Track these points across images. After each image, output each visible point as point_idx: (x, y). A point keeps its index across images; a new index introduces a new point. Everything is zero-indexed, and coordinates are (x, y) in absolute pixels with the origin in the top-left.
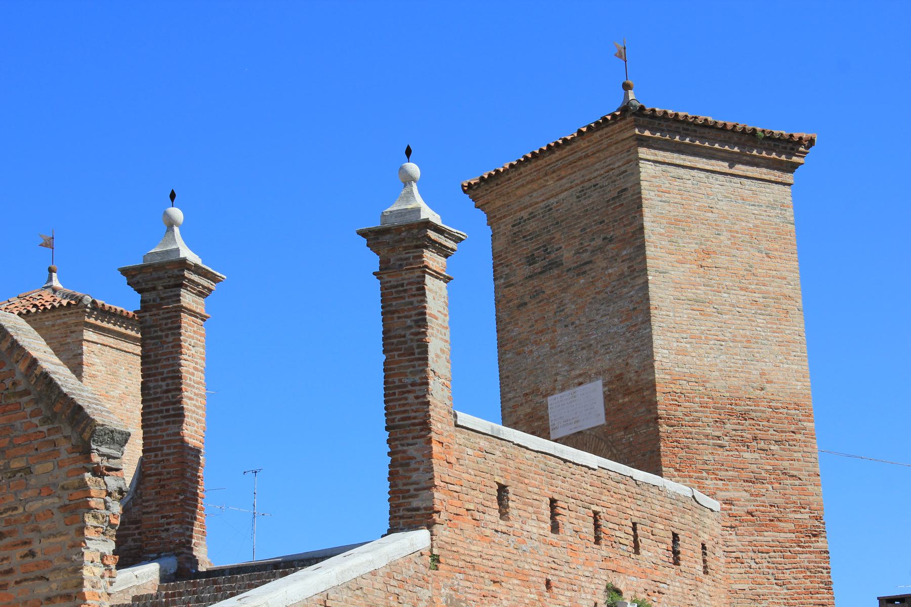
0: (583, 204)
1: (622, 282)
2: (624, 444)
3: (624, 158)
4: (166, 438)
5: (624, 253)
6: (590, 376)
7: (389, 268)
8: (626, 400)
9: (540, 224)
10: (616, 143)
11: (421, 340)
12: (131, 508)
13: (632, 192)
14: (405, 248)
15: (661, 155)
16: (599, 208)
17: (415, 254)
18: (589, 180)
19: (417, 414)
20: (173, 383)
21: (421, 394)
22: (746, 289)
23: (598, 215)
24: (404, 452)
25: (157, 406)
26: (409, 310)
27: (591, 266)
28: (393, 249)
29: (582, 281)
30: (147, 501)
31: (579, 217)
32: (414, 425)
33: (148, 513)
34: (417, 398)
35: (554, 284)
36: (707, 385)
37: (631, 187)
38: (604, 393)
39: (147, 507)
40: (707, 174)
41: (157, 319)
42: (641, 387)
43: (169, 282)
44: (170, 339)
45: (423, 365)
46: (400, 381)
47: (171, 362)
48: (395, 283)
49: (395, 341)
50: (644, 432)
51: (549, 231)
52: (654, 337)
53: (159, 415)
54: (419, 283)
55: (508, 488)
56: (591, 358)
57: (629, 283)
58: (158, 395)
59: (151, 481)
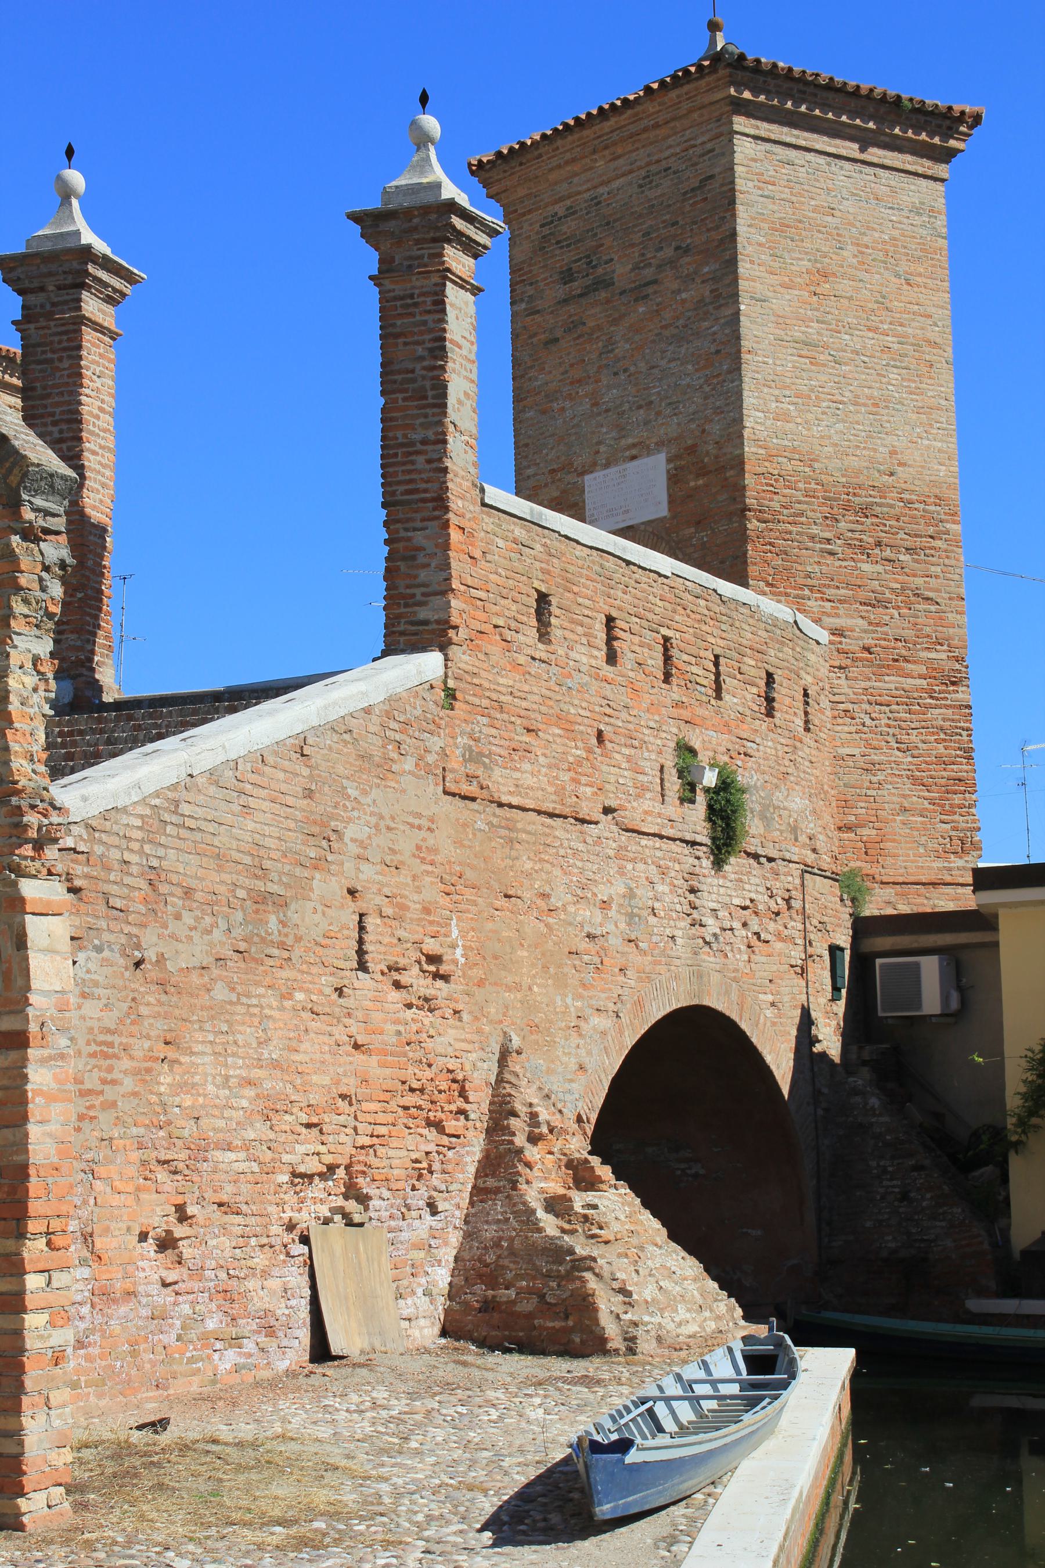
3: (711, 129)
5: (706, 270)
6: (648, 447)
8: (701, 482)
9: (582, 224)
10: (700, 108)
11: (437, 378)
14: (417, 242)
15: (765, 129)
16: (670, 202)
17: (432, 251)
18: (658, 161)
19: (429, 485)
20: (69, 429)
21: (435, 456)
22: (875, 330)
23: (668, 213)
24: (409, 539)
26: (421, 333)
27: (655, 287)
29: (641, 310)
31: (640, 216)
32: (424, 501)
36: (816, 465)
37: (720, 173)
38: (668, 471)
40: (828, 159)
43: (65, 279)
44: (66, 364)
45: (439, 414)
46: (405, 436)
47: (66, 398)
48: (401, 293)
49: (399, 377)
50: (725, 530)
51: (596, 235)
52: (745, 393)
54: (436, 294)
55: (550, 598)
56: (650, 421)
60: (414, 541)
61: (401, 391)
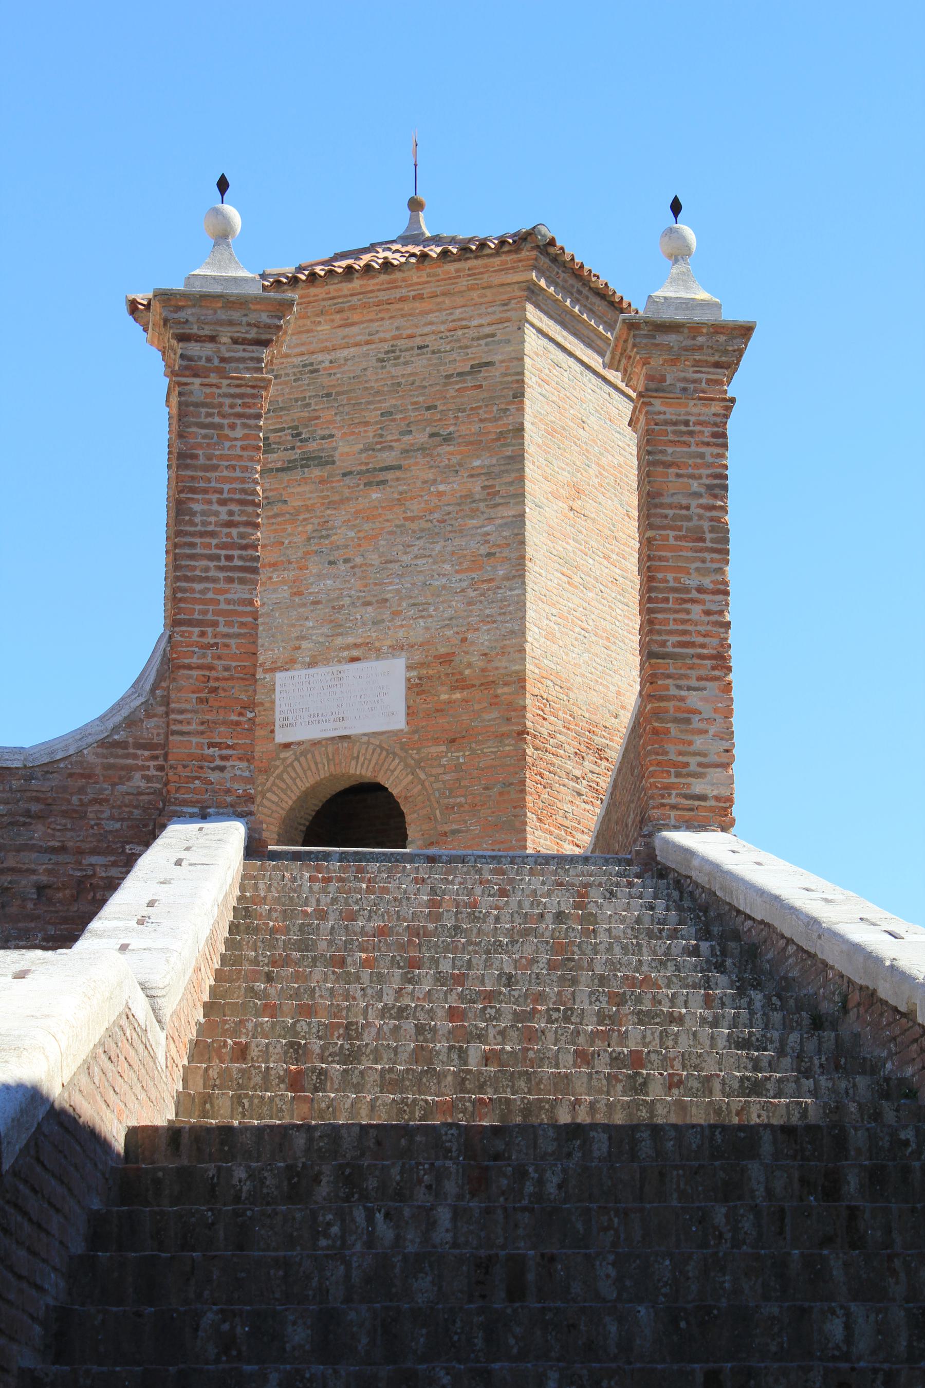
0: (389, 372)
1: (466, 508)
2: (444, 766)
3: (494, 313)
4: (223, 606)
5: (477, 463)
7: (663, 391)
8: (457, 696)
9: (287, 390)
10: (484, 288)
11: (718, 520)
12: (142, 721)
13: (503, 370)
14: (697, 363)
16: (425, 383)
19: (707, 640)
20: (242, 512)
21: (714, 608)
23: (423, 394)
24: (682, 699)
25: (209, 546)
26: (697, 466)
27: (398, 473)
28: (674, 362)
29: (374, 496)
30: (182, 712)
32: (701, 657)
33: (182, 733)
34: (708, 613)
35: (311, 492)
36: (571, 695)
37: (503, 361)
38: (408, 680)
39: (181, 722)
40: (583, 368)
41: (213, 394)
42: (491, 679)
43: (247, 332)
44: (239, 433)
45: (719, 561)
46: (677, 580)
47: (238, 474)
48: (674, 418)
49: (670, 512)
50: (491, 752)
51: (309, 405)
53: (212, 564)
54: (716, 425)
56: (383, 621)
57: (483, 513)
58: (210, 528)
59: (190, 677)
60: (688, 702)
61: (672, 528)
